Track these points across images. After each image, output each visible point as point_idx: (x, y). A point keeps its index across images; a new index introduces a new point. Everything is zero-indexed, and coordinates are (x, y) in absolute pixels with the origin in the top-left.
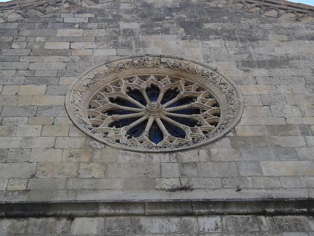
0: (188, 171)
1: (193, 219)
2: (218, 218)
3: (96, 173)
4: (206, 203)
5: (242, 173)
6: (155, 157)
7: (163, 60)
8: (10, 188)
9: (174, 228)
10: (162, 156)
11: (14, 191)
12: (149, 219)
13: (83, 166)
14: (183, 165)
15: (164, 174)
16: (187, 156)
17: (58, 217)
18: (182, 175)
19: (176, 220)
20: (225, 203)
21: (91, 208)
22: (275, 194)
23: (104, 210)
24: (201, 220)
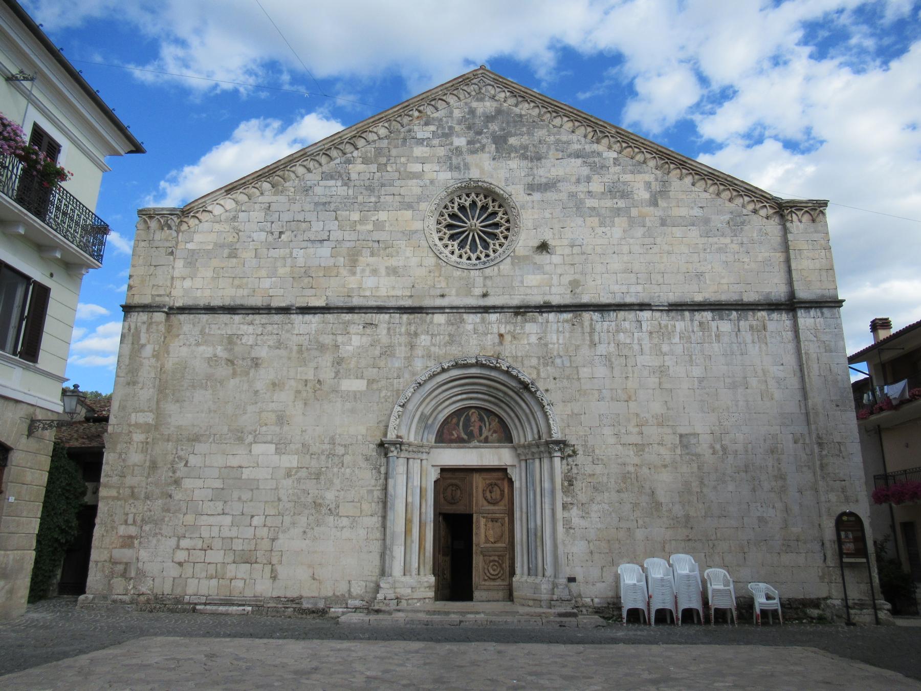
0: (489, 283)
1: (487, 315)
2: (498, 315)
3: (443, 285)
4: (494, 307)
5: (514, 285)
6: (472, 272)
7: (480, 184)
8: (404, 294)
9: (478, 320)
10: (475, 271)
11: (405, 296)
12: (467, 315)
13: (436, 279)
14: (485, 278)
15: (476, 285)
16: (488, 272)
17: (427, 313)
18: (484, 286)
19: (479, 315)
20: (502, 308)
21: (441, 309)
22: (525, 303)
23: (447, 311)
24: (491, 315)
